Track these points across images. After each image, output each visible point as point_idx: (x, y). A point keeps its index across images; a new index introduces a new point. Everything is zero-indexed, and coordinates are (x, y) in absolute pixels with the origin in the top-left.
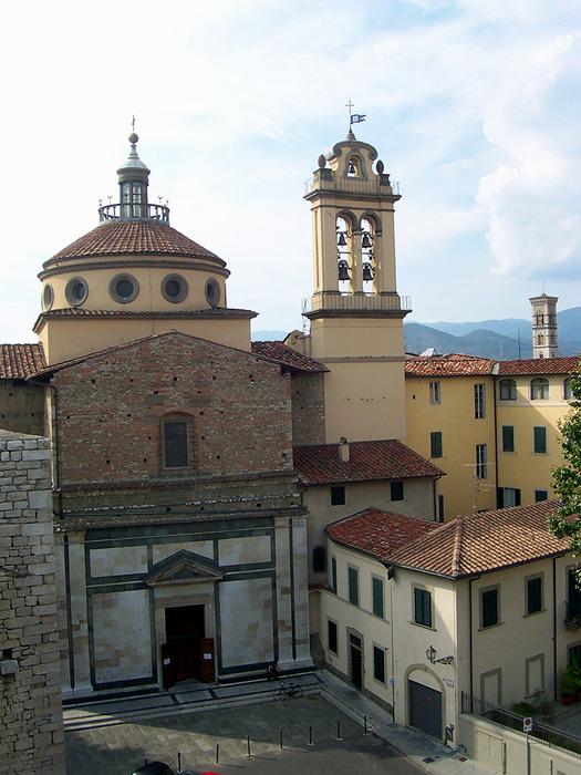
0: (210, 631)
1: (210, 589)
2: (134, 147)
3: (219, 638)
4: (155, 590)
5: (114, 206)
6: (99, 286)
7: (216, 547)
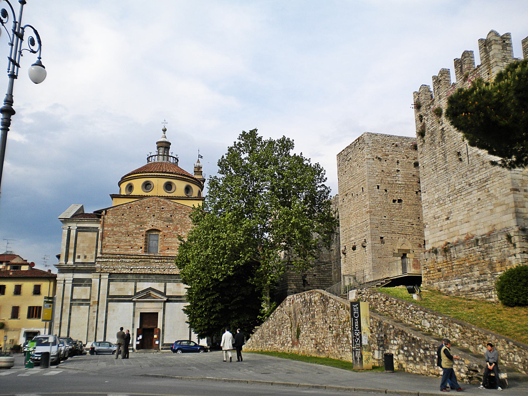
0: (160, 326)
3: (163, 330)
4: (137, 304)
6: (138, 184)
7: (165, 287)
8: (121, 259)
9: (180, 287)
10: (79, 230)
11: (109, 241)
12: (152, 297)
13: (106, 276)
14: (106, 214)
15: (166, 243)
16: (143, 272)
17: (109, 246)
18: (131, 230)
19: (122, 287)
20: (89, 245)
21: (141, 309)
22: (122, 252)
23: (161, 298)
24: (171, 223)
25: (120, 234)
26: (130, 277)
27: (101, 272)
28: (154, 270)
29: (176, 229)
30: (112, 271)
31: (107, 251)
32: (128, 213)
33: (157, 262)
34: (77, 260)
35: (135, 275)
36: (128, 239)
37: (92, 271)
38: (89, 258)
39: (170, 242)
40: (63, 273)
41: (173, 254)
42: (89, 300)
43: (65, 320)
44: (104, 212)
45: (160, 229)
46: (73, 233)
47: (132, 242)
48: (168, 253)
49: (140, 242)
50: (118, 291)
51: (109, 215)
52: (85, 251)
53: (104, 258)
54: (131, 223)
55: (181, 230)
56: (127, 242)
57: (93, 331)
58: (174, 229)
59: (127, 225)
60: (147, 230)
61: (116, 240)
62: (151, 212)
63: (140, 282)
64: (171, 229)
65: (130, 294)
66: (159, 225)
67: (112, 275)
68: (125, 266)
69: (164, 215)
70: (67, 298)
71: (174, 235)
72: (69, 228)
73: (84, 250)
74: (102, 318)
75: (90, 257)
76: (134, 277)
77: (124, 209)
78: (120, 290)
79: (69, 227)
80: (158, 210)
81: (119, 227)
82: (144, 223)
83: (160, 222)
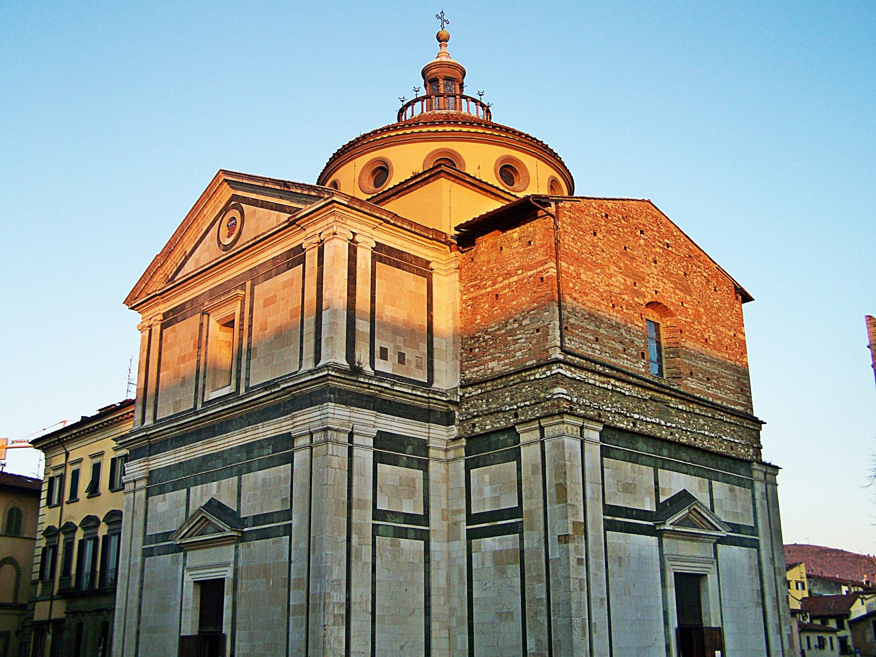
15: (686, 353)
18: (617, 290)
22: (605, 358)
24: (688, 298)
26: (642, 447)
33: (682, 410)
42: (425, 519)
46: (364, 258)
60: (647, 301)
61: (589, 314)
80: (660, 247)
81: (590, 270)
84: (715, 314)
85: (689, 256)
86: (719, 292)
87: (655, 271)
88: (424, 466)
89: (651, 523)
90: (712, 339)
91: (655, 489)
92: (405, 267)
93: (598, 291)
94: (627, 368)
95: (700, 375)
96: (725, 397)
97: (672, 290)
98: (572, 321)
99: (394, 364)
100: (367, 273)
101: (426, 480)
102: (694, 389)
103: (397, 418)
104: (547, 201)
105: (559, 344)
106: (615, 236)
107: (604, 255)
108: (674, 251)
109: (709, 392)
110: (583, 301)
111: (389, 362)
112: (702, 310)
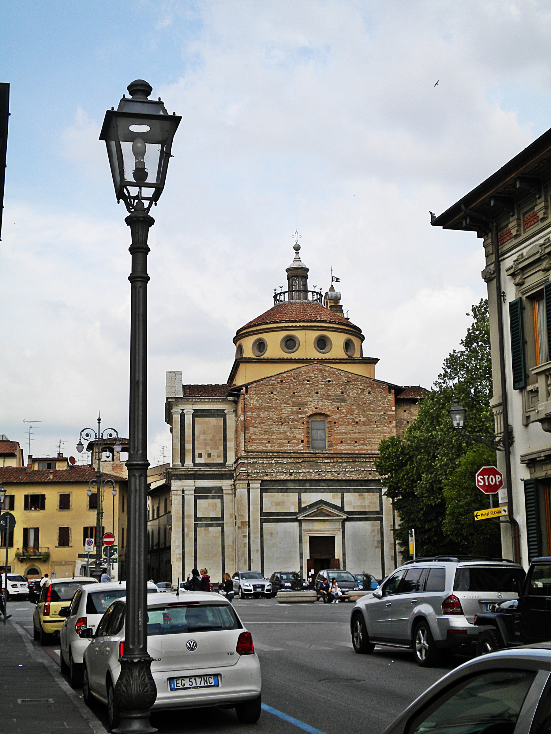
0: (338, 554)
1: (339, 525)
2: (297, 253)
3: (344, 562)
5: (284, 293)
7: (342, 498)
8: (275, 459)
9: (364, 498)
10: (197, 414)
11: (255, 433)
12: (325, 513)
13: (256, 486)
14: (247, 392)
15: (338, 433)
16: (309, 478)
17: (256, 439)
19: (281, 501)
20: (214, 436)
21: (310, 531)
22: (276, 448)
23: (338, 516)
24: (343, 404)
25: (269, 422)
26: (290, 486)
27: (249, 479)
28: (324, 475)
29: (351, 412)
30: (264, 476)
31: (253, 448)
32: (278, 389)
33: (328, 462)
34: (198, 460)
35: (297, 482)
36: (282, 429)
37: (228, 476)
38: (216, 457)
39: (344, 433)
40: (180, 479)
41: (349, 450)
42: (222, 518)
43: (190, 548)
44: (244, 389)
45: (328, 413)
46: (188, 419)
47: (289, 434)
48: (341, 448)
49: (299, 434)
50: (276, 505)
51: (252, 393)
52: (208, 445)
53: (251, 458)
54: (285, 405)
55: (358, 414)
56: (281, 433)
57: (245, 563)
58: (348, 412)
59: (279, 408)
60: (308, 414)
61: (265, 431)
62: (312, 387)
63: (305, 492)
64: (343, 413)
65: (292, 510)
66: (327, 406)
67: (265, 483)
68: (282, 470)
69: (332, 392)
70: (189, 516)
71: (348, 422)
72: (183, 412)
73: (206, 445)
74: (256, 545)
75: (216, 454)
76: (296, 485)
77: (272, 384)
78: (278, 504)
79: (183, 410)
80: (321, 384)
81: (267, 410)
82: (304, 404)
83: (327, 402)
84: (367, 407)
85: (348, 381)
86: (373, 394)
87: (317, 398)
88: (221, 498)
89: (295, 517)
90: (362, 420)
91: (299, 502)
92: (211, 416)
93: (272, 419)
94: (290, 450)
95: (349, 441)
96: (371, 448)
97: (329, 404)
98: (252, 437)
99: (205, 459)
100: (190, 424)
101: (222, 503)
102: (342, 449)
103: (205, 480)
104: (240, 388)
105: (244, 449)
106: (287, 390)
107: (278, 401)
108: (334, 382)
109: (356, 448)
110: (261, 427)
111: (203, 458)
112: (354, 407)
